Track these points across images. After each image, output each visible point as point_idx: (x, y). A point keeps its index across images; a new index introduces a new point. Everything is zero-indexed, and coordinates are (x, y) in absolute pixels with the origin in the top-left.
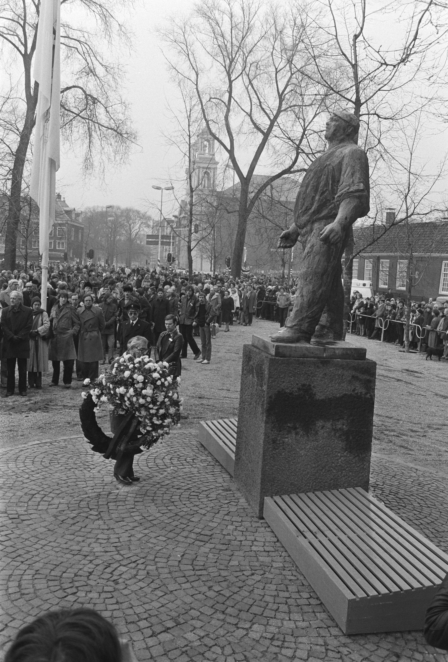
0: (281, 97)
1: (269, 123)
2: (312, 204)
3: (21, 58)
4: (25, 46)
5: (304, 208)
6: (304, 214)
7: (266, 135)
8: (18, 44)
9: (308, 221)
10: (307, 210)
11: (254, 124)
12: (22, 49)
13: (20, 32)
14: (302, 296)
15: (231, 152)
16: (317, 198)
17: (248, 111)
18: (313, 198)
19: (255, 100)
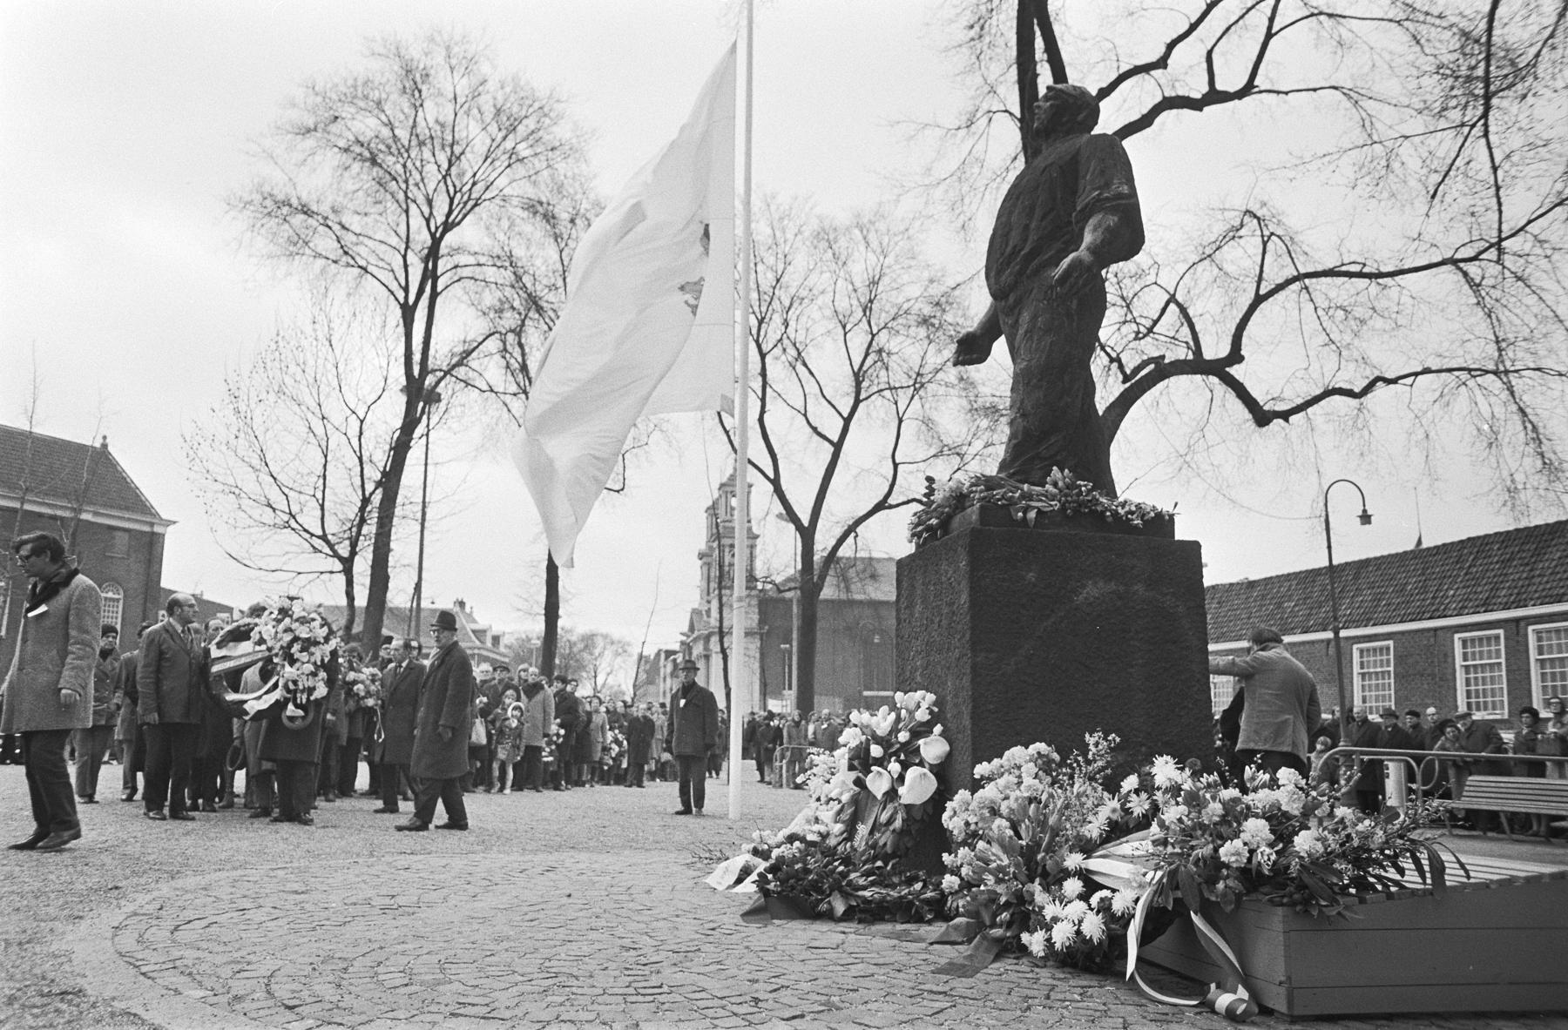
0: (858, 377)
1: (841, 423)
2: (1025, 240)
3: (399, 312)
4: (406, 289)
5: (1009, 249)
6: (1008, 264)
7: (838, 447)
8: (394, 286)
9: (1020, 273)
10: (1015, 252)
11: (815, 429)
12: (401, 295)
13: (397, 262)
14: (1023, 415)
15: (776, 482)
16: (1033, 226)
17: (799, 405)
18: (1027, 227)
19: (811, 388)
